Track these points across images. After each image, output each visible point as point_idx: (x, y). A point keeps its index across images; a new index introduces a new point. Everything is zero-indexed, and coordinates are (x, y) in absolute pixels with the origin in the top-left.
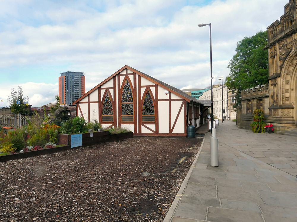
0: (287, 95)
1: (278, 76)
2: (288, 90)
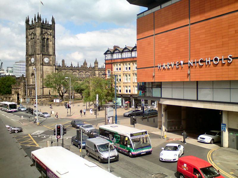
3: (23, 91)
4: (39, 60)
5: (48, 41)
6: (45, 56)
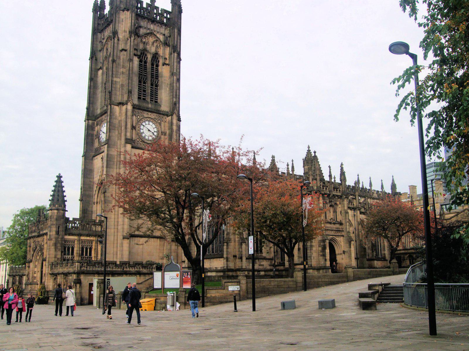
0: (35, 275)
1: (31, 261)
2: (36, 272)
3: (55, 245)
4: (123, 124)
5: (157, 66)
6: (146, 114)
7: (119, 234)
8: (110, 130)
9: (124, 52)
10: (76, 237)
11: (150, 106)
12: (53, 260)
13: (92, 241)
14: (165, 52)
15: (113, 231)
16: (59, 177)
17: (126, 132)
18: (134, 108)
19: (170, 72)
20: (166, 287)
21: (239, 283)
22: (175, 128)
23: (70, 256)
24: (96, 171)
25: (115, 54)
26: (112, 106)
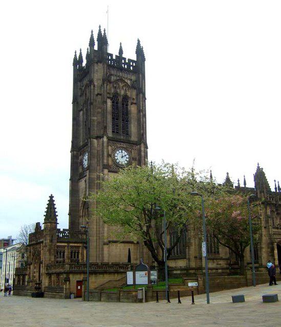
0: (35, 275)
1: (32, 264)
3: (49, 250)
4: (101, 153)
5: (127, 105)
7: (101, 240)
8: (90, 159)
9: (99, 96)
10: (66, 244)
11: (122, 137)
12: (47, 262)
13: (79, 246)
14: (132, 94)
15: (95, 238)
16: (51, 197)
17: (103, 159)
18: (109, 140)
19: (138, 109)
20: (137, 283)
21: (197, 280)
22: (143, 154)
23: (62, 259)
24: (81, 191)
25: (92, 98)
26: (92, 139)
